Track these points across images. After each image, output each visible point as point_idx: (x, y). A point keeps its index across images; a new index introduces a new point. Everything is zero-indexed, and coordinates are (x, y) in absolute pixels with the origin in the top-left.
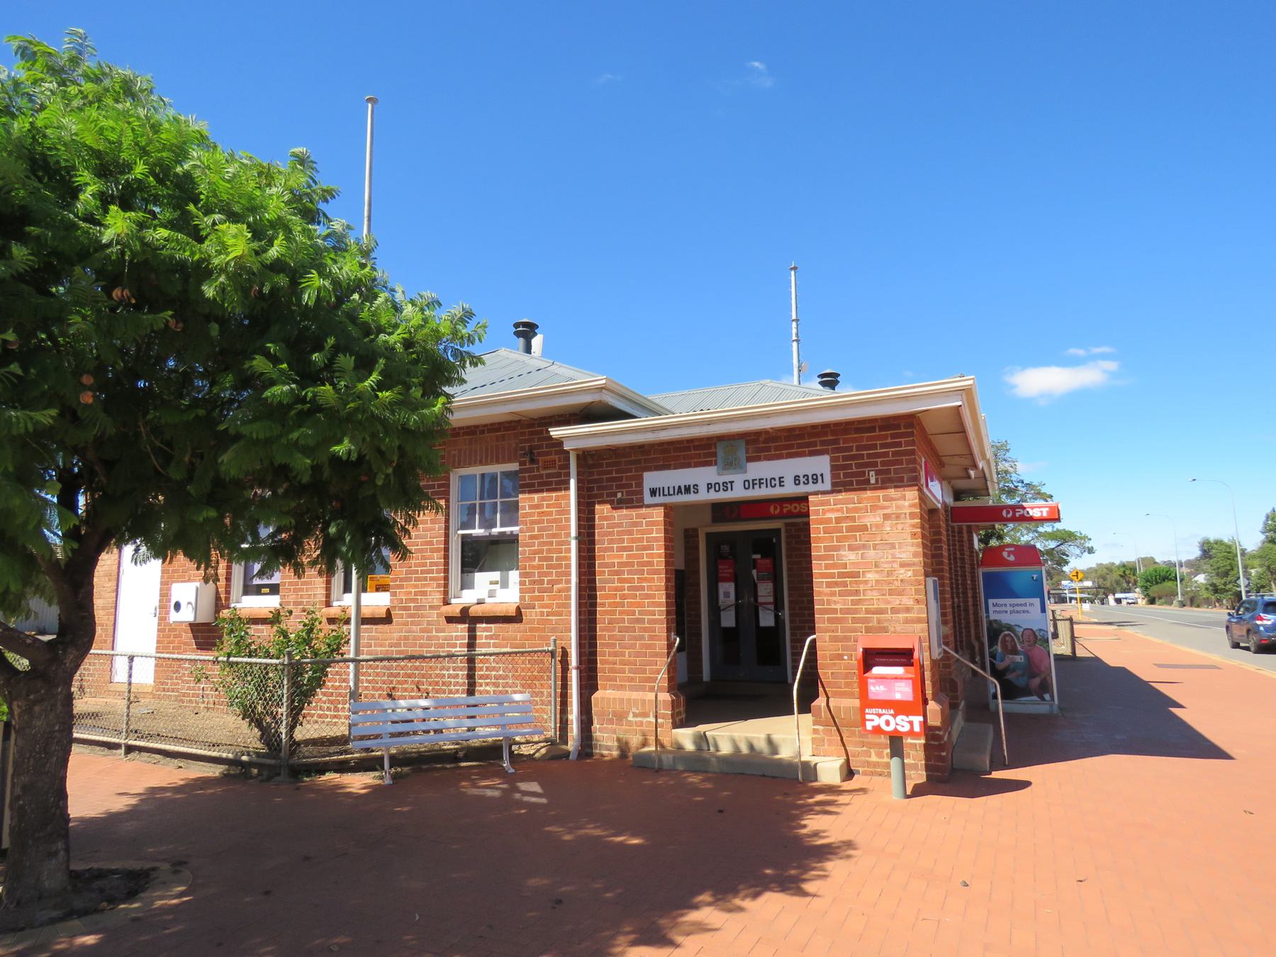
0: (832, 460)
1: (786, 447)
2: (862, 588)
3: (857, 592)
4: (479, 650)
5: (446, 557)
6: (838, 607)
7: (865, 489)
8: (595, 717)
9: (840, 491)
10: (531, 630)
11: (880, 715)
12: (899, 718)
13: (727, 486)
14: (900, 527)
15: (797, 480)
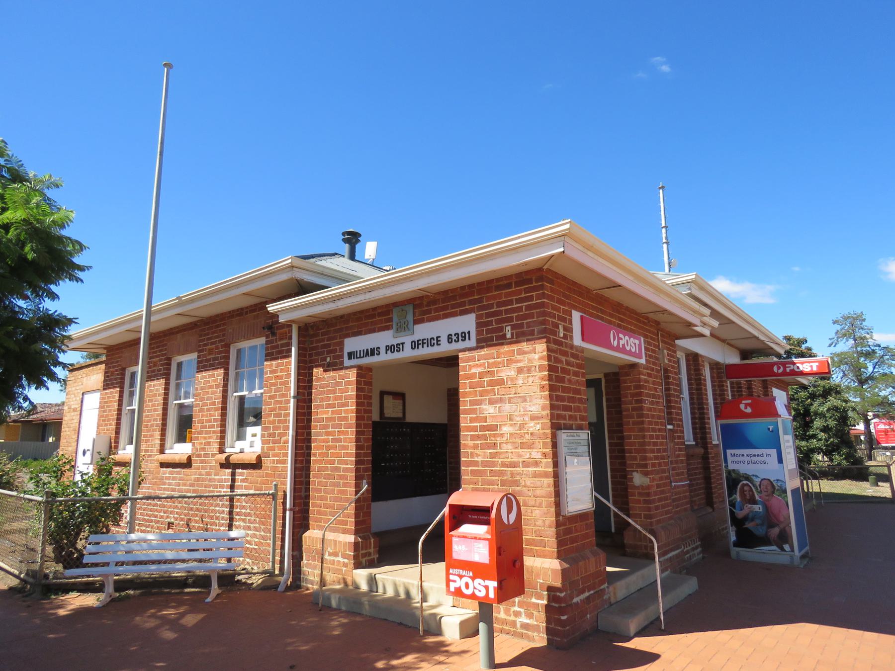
0: (478, 317)
1: (443, 309)
2: (499, 440)
3: (494, 445)
4: (238, 491)
5: (224, 415)
6: (480, 459)
7: (502, 344)
8: (304, 554)
9: (482, 347)
10: (267, 475)
11: (461, 577)
12: (478, 581)
13: (400, 347)
14: (531, 380)
15: (450, 339)
